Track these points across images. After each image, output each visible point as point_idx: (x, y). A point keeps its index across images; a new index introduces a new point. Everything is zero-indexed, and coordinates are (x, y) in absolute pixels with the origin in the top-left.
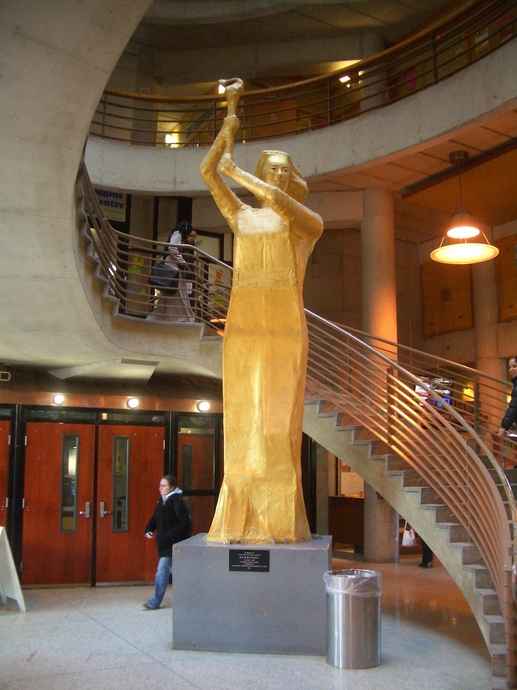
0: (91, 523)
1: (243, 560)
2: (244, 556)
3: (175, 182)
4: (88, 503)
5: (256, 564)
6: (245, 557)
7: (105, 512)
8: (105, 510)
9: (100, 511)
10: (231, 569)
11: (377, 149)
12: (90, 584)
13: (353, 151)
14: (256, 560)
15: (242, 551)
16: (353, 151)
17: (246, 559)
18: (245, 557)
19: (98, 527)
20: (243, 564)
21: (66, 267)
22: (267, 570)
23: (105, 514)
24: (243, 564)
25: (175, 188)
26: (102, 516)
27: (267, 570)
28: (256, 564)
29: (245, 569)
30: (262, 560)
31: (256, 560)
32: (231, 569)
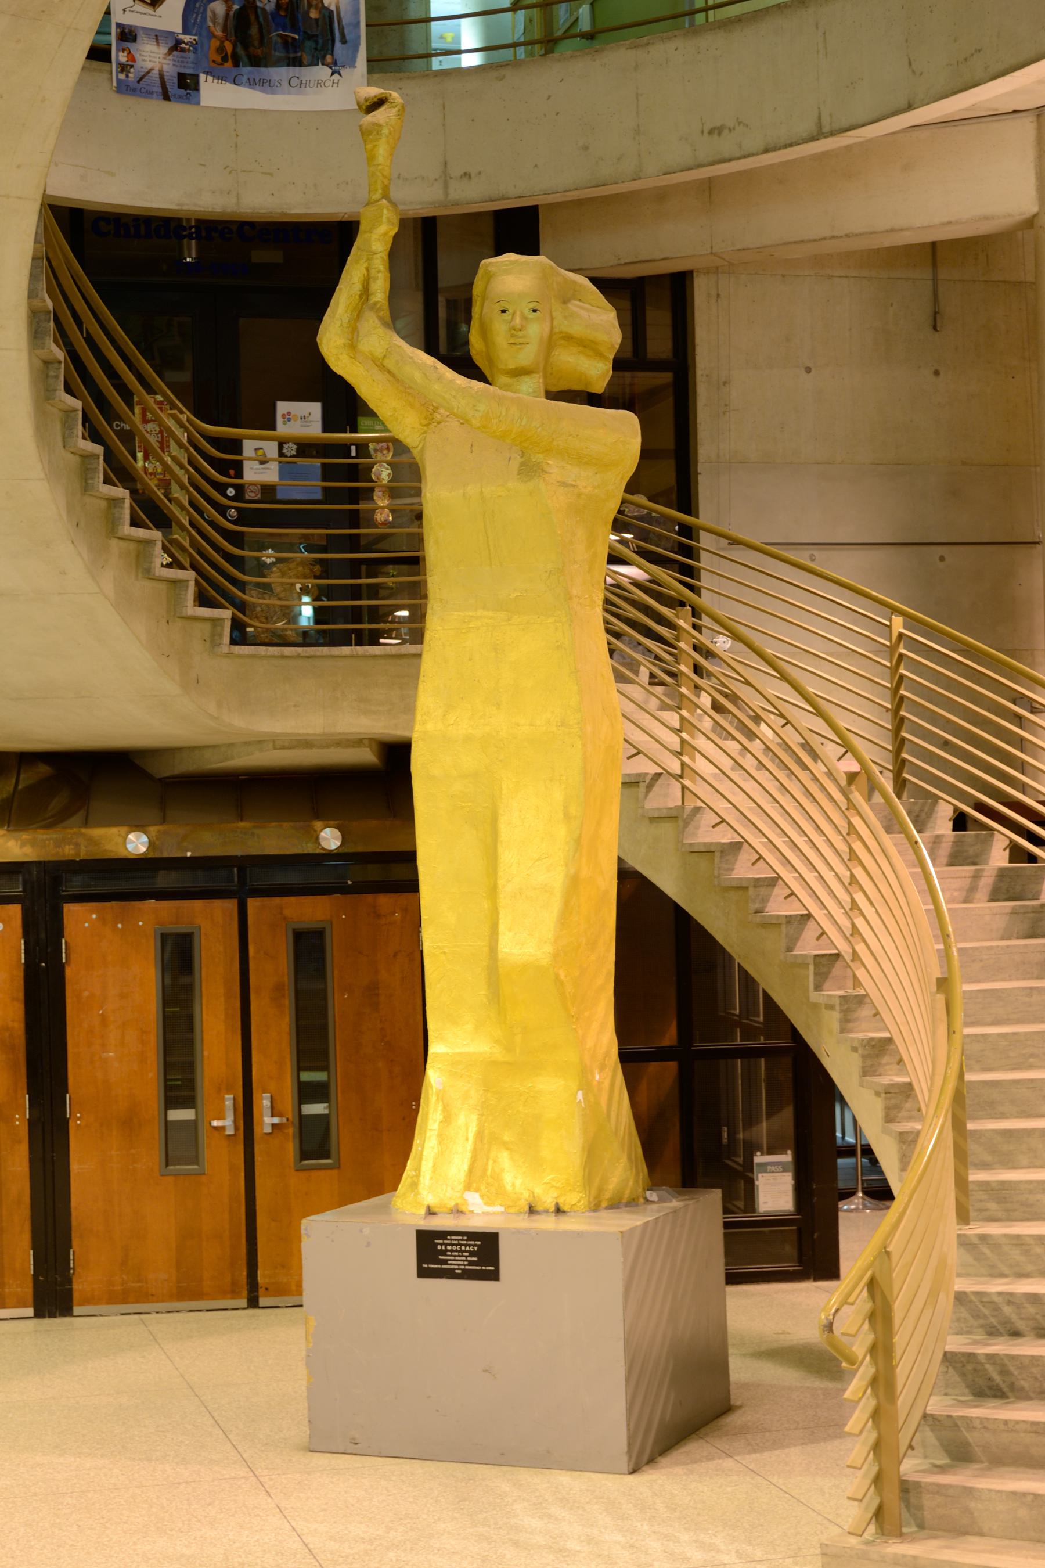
0: (241, 1148)
1: (444, 1253)
2: (446, 1245)
3: (446, 179)
4: (228, 1101)
5: (471, 1263)
6: (449, 1248)
7: (276, 1120)
8: (272, 1116)
9: (262, 1116)
10: (422, 1273)
11: (966, 60)
12: (244, 1303)
13: (910, 63)
14: (472, 1254)
15: (443, 1234)
16: (910, 63)
17: (452, 1251)
18: (449, 1248)
19: (258, 1159)
20: (445, 1262)
21: (63, 573)
22: (494, 1276)
23: (273, 1125)
24: (445, 1262)
25: (446, 194)
26: (268, 1130)
27: (494, 1276)
28: (471, 1263)
29: (451, 1274)
30: (483, 1254)
31: (472, 1254)
32: (422, 1273)
